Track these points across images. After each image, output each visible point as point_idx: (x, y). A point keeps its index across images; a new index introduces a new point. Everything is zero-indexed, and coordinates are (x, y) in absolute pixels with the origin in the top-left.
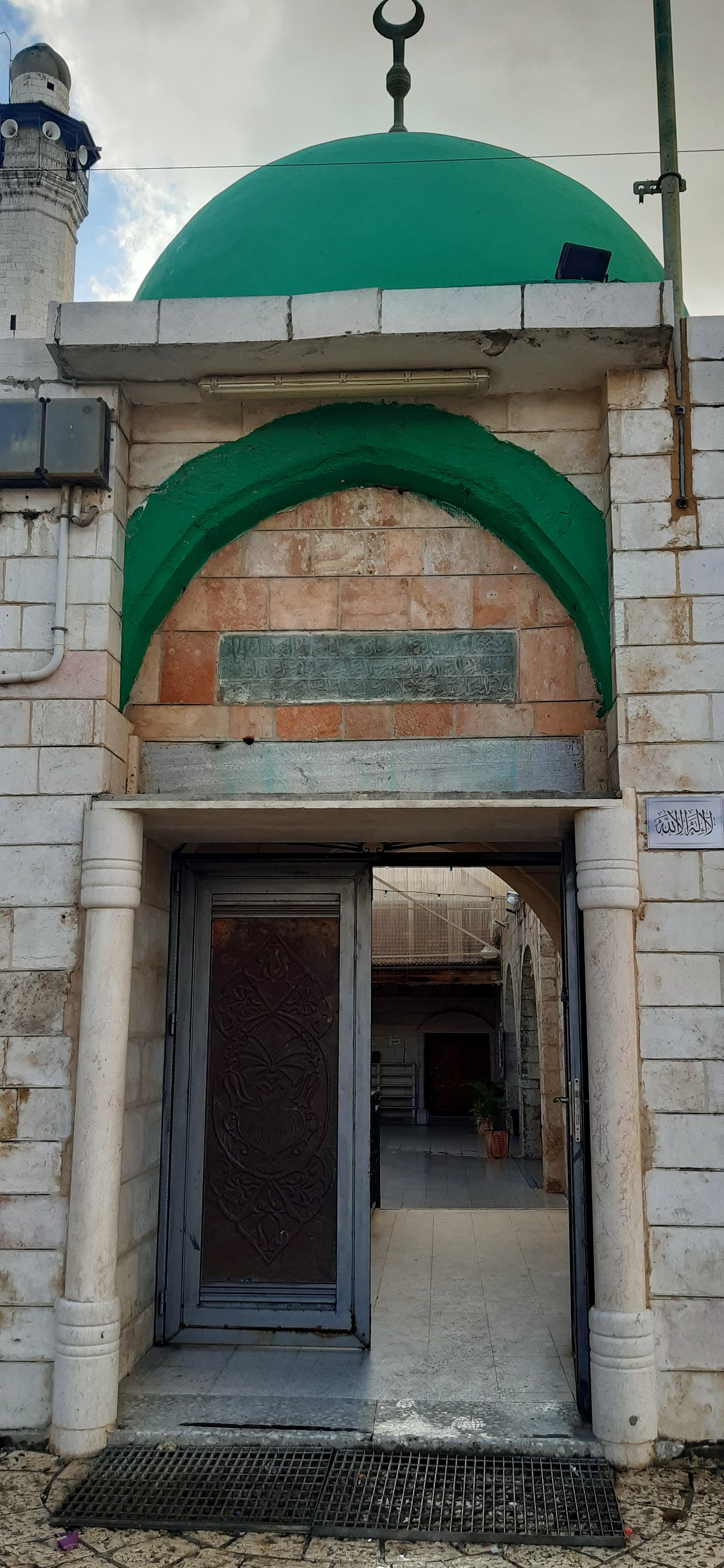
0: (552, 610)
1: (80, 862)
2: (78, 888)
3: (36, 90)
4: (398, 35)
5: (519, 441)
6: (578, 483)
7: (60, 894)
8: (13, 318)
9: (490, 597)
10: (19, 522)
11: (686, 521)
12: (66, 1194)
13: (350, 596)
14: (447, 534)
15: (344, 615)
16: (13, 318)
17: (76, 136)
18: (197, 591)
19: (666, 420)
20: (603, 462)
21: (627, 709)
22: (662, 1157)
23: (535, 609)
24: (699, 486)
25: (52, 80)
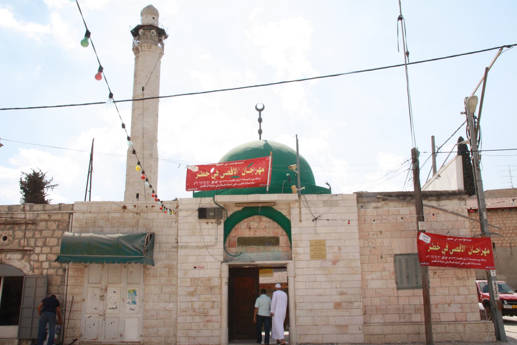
0: (284, 233)
1: (221, 271)
2: (220, 275)
3: (149, 21)
4: (260, 111)
5: (279, 210)
6: (287, 217)
7: (218, 275)
8: (143, 88)
9: (276, 231)
10: (210, 224)
11: (301, 224)
12: (221, 315)
13: (256, 231)
14: (269, 222)
15: (255, 234)
16: (143, 88)
17: (161, 33)
18: (233, 230)
19: (298, 209)
20: (290, 215)
21: (293, 249)
22: (298, 308)
23: (282, 233)
24: (303, 219)
25: (154, 16)
